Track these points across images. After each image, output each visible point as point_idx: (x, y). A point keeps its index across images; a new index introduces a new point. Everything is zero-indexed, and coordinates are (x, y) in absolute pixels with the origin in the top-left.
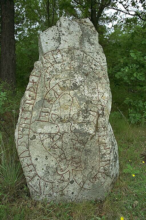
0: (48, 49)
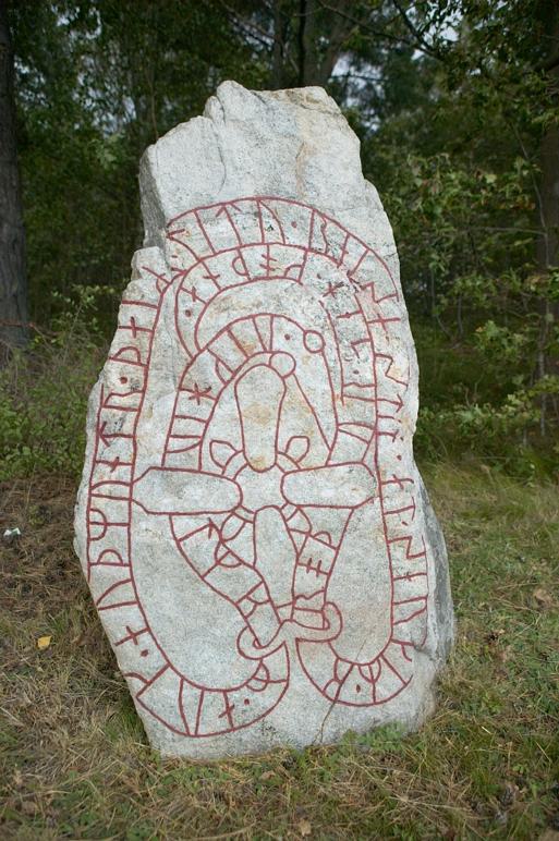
0: (183, 203)
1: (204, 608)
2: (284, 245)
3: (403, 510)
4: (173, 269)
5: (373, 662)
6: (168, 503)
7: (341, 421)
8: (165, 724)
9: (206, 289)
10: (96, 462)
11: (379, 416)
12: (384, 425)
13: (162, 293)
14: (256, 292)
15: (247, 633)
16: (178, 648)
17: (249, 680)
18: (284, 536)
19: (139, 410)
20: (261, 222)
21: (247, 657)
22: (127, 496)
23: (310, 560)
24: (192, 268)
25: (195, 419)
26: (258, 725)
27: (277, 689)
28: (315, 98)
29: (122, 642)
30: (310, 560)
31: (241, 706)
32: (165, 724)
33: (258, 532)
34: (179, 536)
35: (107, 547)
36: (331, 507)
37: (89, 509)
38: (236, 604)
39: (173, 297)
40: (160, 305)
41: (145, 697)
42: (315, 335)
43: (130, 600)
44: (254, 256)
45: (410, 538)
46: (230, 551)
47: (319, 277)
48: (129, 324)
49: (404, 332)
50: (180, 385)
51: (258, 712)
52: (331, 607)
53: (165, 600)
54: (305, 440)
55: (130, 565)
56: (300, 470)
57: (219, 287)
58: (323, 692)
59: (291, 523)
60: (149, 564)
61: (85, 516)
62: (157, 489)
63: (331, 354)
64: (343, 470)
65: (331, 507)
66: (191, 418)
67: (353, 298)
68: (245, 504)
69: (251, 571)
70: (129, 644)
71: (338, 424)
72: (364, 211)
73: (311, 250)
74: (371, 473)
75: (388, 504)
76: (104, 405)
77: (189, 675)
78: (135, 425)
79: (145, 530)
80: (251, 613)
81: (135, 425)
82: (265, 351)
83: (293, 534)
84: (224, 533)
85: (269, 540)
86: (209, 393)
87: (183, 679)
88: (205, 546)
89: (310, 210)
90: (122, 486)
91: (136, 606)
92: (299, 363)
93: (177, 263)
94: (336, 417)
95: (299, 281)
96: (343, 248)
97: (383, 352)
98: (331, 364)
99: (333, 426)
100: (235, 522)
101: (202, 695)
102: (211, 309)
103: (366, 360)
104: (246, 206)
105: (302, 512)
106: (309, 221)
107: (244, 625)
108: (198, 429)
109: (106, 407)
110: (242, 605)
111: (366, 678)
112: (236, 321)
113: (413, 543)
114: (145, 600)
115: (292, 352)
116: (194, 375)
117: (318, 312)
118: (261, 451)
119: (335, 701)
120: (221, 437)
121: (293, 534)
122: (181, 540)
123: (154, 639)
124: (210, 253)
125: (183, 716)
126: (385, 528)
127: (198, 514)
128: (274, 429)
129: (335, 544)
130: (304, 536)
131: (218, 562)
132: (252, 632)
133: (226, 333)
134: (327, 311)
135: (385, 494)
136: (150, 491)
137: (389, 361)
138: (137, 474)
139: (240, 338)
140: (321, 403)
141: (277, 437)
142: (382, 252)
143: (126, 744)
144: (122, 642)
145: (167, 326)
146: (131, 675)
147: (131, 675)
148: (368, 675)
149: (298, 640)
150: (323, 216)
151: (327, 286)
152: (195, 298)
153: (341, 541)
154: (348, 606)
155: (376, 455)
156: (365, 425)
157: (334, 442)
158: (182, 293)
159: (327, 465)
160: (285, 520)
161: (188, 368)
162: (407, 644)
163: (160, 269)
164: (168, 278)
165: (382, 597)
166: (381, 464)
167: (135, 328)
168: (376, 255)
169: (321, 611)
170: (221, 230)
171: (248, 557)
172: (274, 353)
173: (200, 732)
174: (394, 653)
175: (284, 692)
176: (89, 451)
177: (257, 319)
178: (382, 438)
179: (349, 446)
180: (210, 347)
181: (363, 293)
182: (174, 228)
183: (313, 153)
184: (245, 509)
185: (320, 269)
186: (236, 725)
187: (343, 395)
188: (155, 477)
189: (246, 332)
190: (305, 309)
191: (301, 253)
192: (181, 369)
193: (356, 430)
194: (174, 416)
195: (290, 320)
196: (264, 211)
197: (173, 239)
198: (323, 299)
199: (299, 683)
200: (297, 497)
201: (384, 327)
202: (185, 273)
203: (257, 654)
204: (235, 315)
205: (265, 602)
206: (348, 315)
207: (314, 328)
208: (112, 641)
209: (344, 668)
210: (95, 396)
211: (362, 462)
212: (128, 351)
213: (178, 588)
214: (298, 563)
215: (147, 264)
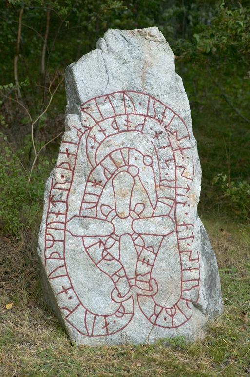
1: (97, 279)
2: (135, 114)
3: (188, 238)
4: (85, 127)
5: (172, 308)
6: (81, 232)
7: (159, 197)
8: (78, 330)
9: (100, 136)
10: (49, 213)
11: (177, 195)
12: (179, 199)
14: (122, 137)
15: (115, 290)
16: (85, 296)
17: (116, 312)
18: (132, 247)
19: (69, 190)
20: (125, 103)
23: (144, 259)
24: (93, 126)
25: (94, 195)
26: (119, 333)
27: (128, 317)
28: (152, 34)
29: (60, 293)
30: (144, 259)
31: (112, 324)
32: (78, 330)
33: (121, 245)
34: (86, 246)
35: (54, 251)
36: (154, 235)
37: (46, 234)
38: (111, 277)
39: (85, 140)
40: (79, 143)
41: (69, 318)
42: (148, 158)
43: (64, 274)
44: (121, 120)
45: (191, 251)
46: (109, 253)
47: (151, 129)
48: (65, 152)
49: (194, 154)
50: (88, 179)
51: (119, 327)
52: (153, 280)
53: (79, 274)
54: (142, 205)
55: (64, 259)
56: (140, 218)
57: (105, 135)
58: (149, 320)
60: (73, 258)
61: (44, 237)
62: (77, 226)
63: (156, 166)
64: (160, 219)
65: (154, 235)
66: (92, 194)
67: (167, 139)
68: (116, 232)
69: (117, 262)
70: (63, 295)
71: (158, 198)
72: (174, 94)
73: (148, 116)
74: (172, 220)
75: (180, 235)
77: (89, 308)
78: (67, 197)
79: (71, 243)
80: (118, 281)
81: (67, 197)
82: (126, 165)
83: (137, 246)
84: (106, 245)
85: (126, 249)
86: (101, 183)
87: (87, 310)
88: (98, 251)
89: (148, 96)
90: (61, 224)
91: (67, 277)
92: (141, 170)
93: (86, 124)
94: (157, 195)
95: (141, 132)
96: (163, 114)
97: (180, 165)
98: (155, 171)
99: (155, 199)
100: (111, 241)
101: (95, 318)
102: (102, 146)
103: (172, 168)
104: (118, 95)
105: (141, 237)
106: (147, 102)
107: (114, 287)
108: (95, 199)
109: (54, 188)
110: (113, 277)
111: (169, 315)
112: (113, 151)
113: (192, 254)
114: (71, 274)
115: (138, 165)
116: (94, 175)
117: (150, 147)
118: (123, 209)
119: (155, 324)
120: (106, 203)
121: (137, 246)
122: (87, 248)
123: (74, 291)
124: (101, 119)
125: (86, 327)
126: (179, 246)
127: (95, 236)
128: (129, 200)
129: (156, 252)
130: (141, 248)
131: (103, 258)
132: (118, 290)
133: (108, 157)
134: (154, 146)
135: (179, 231)
136: (75, 227)
137: (183, 169)
138: (68, 219)
139: (115, 159)
140: (150, 189)
141: (130, 203)
142: (182, 115)
143: (61, 340)
144: (60, 293)
145: (82, 153)
147: (63, 308)
148: (170, 313)
149: (138, 295)
150: (154, 99)
151: (155, 134)
152: (95, 141)
153: (158, 251)
154: (161, 281)
155: (175, 213)
156: (170, 199)
157: (156, 206)
158: (89, 138)
159: (152, 216)
160: (133, 240)
161: (91, 172)
162: (189, 301)
163: (79, 126)
164: (83, 131)
165: (177, 277)
166: (177, 217)
167: (68, 153)
168: (179, 117)
169: (149, 282)
170: (106, 108)
171: (116, 256)
172: (129, 166)
173: (93, 335)
174: (182, 304)
175: (131, 319)
177: (122, 151)
178: (178, 204)
179: (163, 208)
180: (102, 163)
181: (172, 136)
182: (85, 106)
183: (150, 66)
184: (116, 235)
185: (152, 125)
188: (76, 220)
189: (117, 156)
190: (144, 145)
191: (143, 118)
192: (88, 172)
193: (166, 201)
194: (85, 193)
195: (137, 151)
196: (127, 98)
197: (84, 112)
198: (153, 140)
199: (138, 315)
200: (138, 230)
202: (90, 129)
203: (120, 300)
204: (113, 148)
205: (124, 277)
206: (164, 147)
209: (159, 309)
210: (49, 183)
211: (168, 215)
212: (65, 164)
213: (85, 269)
215: (73, 124)
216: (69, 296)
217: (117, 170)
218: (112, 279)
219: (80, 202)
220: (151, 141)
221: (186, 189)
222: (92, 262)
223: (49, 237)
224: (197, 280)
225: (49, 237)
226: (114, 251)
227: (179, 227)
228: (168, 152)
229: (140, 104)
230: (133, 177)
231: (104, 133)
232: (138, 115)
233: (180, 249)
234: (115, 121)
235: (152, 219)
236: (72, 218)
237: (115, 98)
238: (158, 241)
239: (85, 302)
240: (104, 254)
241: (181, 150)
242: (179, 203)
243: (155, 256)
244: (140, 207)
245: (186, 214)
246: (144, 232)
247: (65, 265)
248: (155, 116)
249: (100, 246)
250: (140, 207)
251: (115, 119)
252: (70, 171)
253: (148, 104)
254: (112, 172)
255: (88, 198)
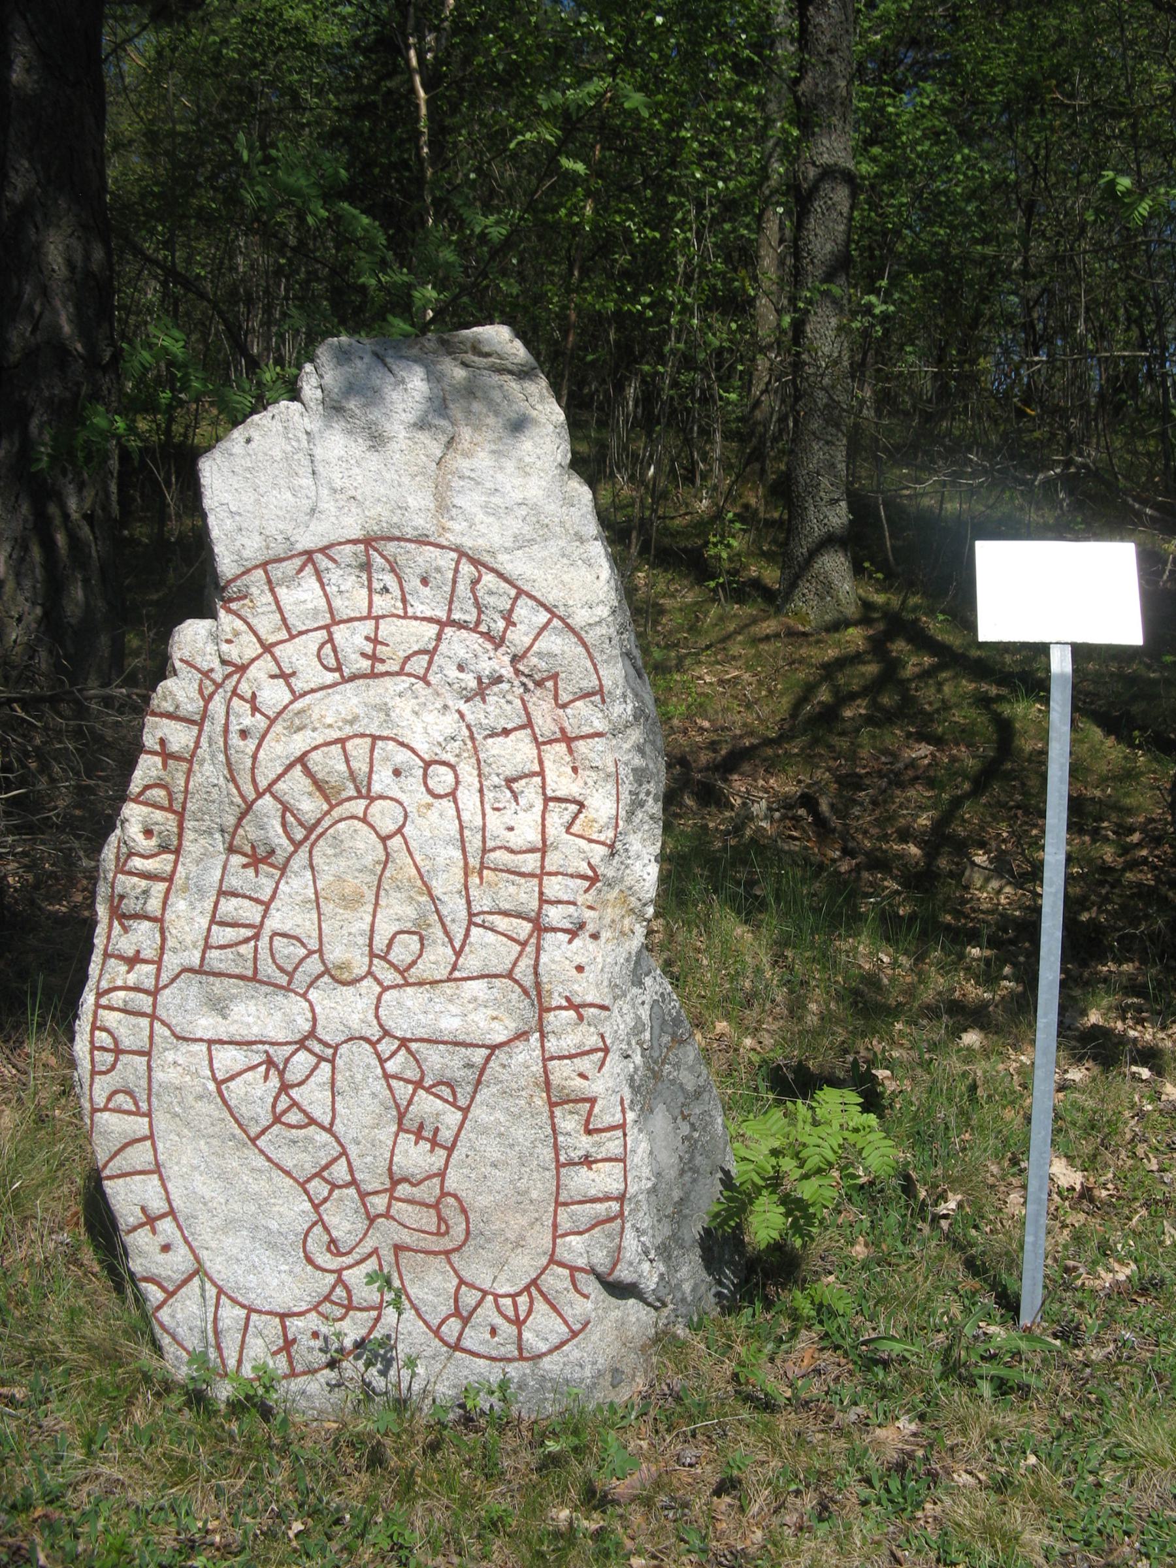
0: (246, 553)
5: (519, 1294)
6: (206, 1025)
9: (274, 695)
10: (107, 955)
11: (543, 900)
12: (554, 915)
13: (208, 700)
14: (348, 701)
16: (213, 1244)
17: (320, 1303)
18: (380, 1086)
20: (370, 580)
21: (318, 1268)
22: (149, 1011)
23: (421, 1127)
24: (253, 660)
28: (486, 349)
30: (421, 1127)
33: (339, 1077)
37: (94, 1027)
40: (203, 719)
42: (443, 769)
44: (352, 639)
45: (592, 1101)
46: (295, 1104)
47: (461, 668)
52: (451, 1200)
55: (149, 1114)
56: (408, 984)
57: (293, 692)
58: (437, 1332)
59: (391, 1066)
67: (518, 702)
68: (320, 1031)
69: (325, 1137)
71: (471, 915)
74: (526, 992)
75: (552, 1045)
76: (121, 869)
80: (326, 1200)
82: (360, 796)
83: (393, 1083)
84: (287, 1075)
86: (272, 860)
89: (454, 555)
92: (413, 815)
93: (232, 652)
94: (469, 902)
95: (424, 679)
100: (303, 1060)
101: (248, 1318)
102: (278, 728)
105: (409, 1050)
106: (450, 575)
107: (315, 1218)
108: (252, 913)
110: (310, 1186)
112: (316, 748)
113: (596, 1110)
116: (250, 830)
120: (286, 928)
121: (393, 1083)
128: (369, 919)
130: (410, 1087)
131: (277, 1120)
134: (468, 727)
136: (183, 1005)
137: (574, 808)
138: (165, 978)
139: (319, 776)
140: (446, 884)
141: (372, 930)
142: (580, 618)
145: (213, 756)
146: (147, 1279)
147: (147, 1279)
148: (511, 1313)
149: (398, 1248)
151: (473, 684)
152: (255, 709)
153: (473, 1098)
155: (536, 966)
156: (519, 916)
160: (382, 1061)
161: (240, 819)
162: (581, 1270)
163: (210, 661)
165: (540, 1188)
167: (166, 755)
168: (568, 625)
169: (436, 1206)
170: (302, 597)
174: (556, 1281)
176: (99, 941)
178: (549, 936)
181: (538, 692)
184: (320, 1041)
186: (299, 1368)
187: (483, 866)
189: (329, 763)
191: (433, 629)
192: (231, 820)
193: (502, 923)
196: (378, 560)
197: (229, 611)
198: (464, 707)
201: (570, 751)
202: (242, 669)
205: (347, 1185)
206: (506, 732)
207: (445, 757)
208: (122, 1226)
210: (109, 853)
211: (510, 975)
214: (401, 1128)
216: (161, 1240)
217: (327, 813)
218: (306, 1192)
219: (204, 922)
220: (459, 712)
221: (584, 877)
222: (238, 1131)
223: (102, 1038)
224: (616, 1199)
225: (101, 1036)
226: (313, 1097)
227: (550, 1017)
228: (516, 752)
229: (425, 581)
230: (384, 839)
231: (289, 685)
232: (416, 618)
233: (554, 1092)
234: (331, 640)
235: (449, 988)
236: (178, 976)
237: (334, 561)
238: (469, 1066)
239: (215, 1266)
240: (281, 1107)
241: (568, 739)
242: (555, 930)
243: (459, 1115)
244: (407, 946)
245: (580, 969)
246: (421, 1033)
247: (151, 1137)
248: (478, 622)
249: (266, 1078)
250: (407, 946)
251: (330, 634)
252: (171, 816)
253: (454, 582)
254: (310, 819)
255: (229, 907)
